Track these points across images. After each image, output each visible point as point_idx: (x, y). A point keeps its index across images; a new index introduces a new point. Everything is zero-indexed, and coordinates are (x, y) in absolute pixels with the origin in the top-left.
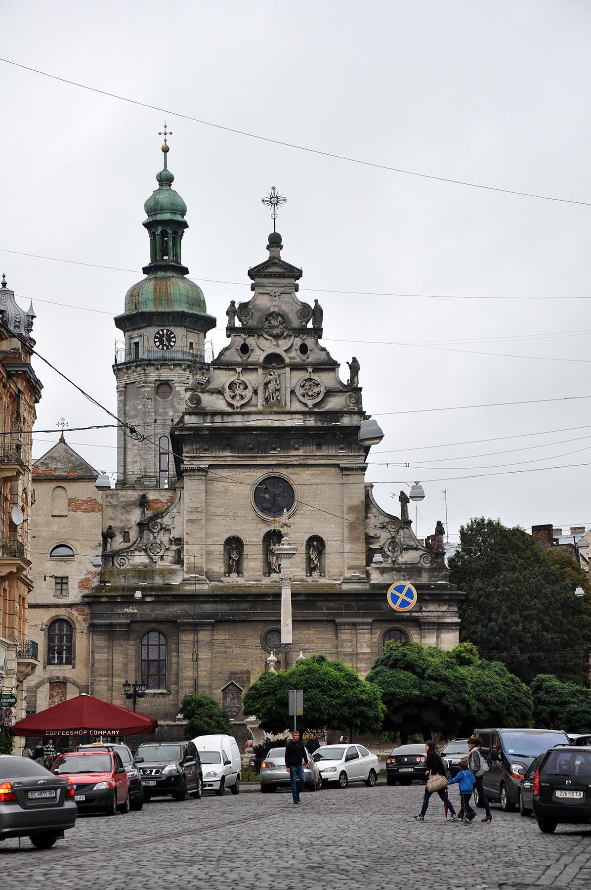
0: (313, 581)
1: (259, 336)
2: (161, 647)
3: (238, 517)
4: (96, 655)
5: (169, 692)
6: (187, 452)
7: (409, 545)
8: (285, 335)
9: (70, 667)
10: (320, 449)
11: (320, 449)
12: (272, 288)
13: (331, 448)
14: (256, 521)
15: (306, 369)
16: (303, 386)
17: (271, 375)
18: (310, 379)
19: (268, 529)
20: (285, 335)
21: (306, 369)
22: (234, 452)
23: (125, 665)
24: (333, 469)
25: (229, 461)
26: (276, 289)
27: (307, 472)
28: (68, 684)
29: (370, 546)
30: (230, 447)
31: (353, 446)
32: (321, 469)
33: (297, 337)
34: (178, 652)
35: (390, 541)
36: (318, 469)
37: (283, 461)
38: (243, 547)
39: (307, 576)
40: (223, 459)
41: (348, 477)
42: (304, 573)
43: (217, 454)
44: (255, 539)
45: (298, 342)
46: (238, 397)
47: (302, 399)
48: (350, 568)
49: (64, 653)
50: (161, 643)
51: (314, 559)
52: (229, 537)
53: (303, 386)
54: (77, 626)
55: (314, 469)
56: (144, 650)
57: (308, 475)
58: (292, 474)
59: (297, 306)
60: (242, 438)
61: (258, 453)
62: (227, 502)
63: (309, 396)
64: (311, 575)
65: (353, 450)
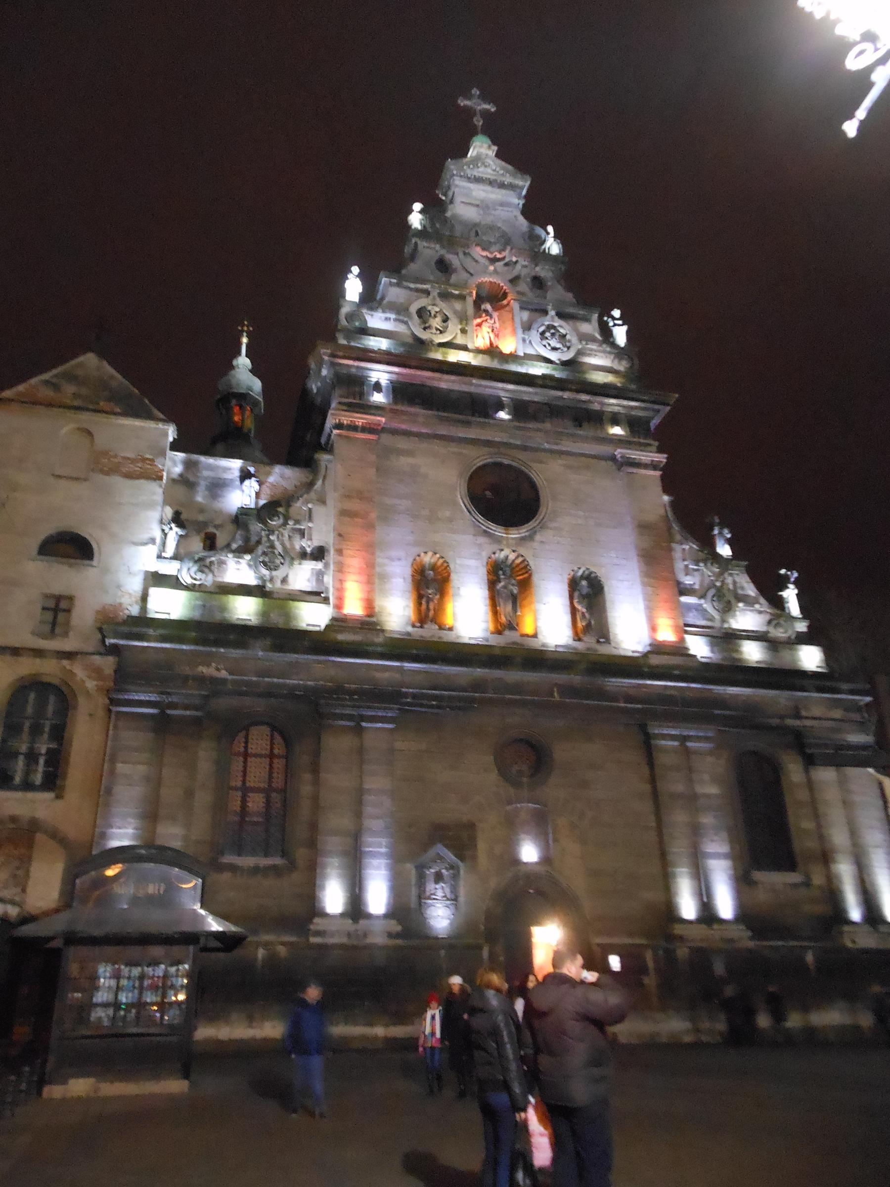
2: (276, 761)
4: (119, 766)
5: (292, 866)
6: (341, 396)
9: (49, 795)
10: (580, 426)
11: (580, 426)
18: (554, 327)
22: (431, 409)
23: (189, 794)
24: (603, 463)
27: (560, 462)
28: (40, 837)
34: (315, 769)
49: (42, 761)
50: (276, 751)
54: (82, 700)
56: (237, 765)
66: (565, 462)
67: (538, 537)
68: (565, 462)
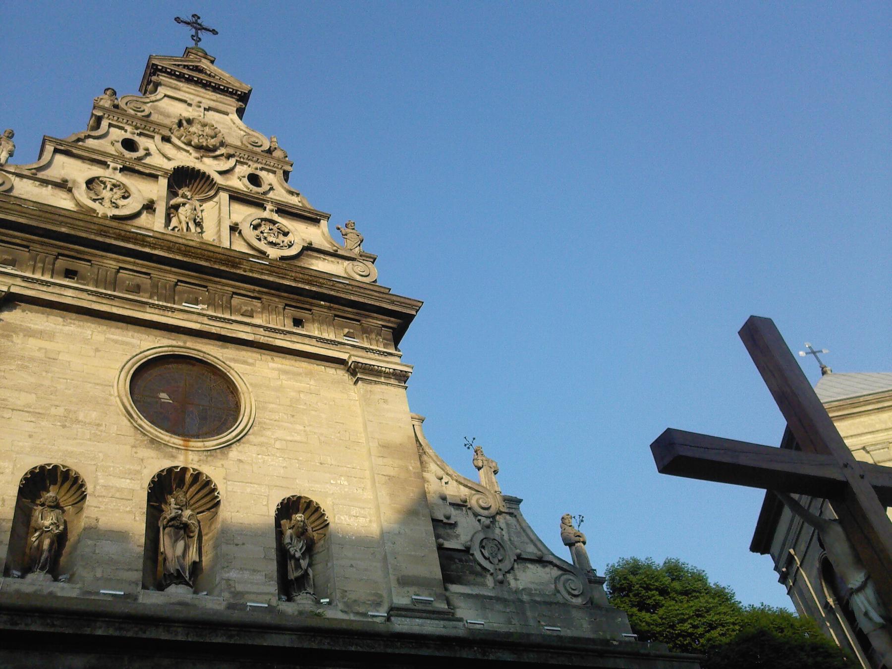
0: (301, 613)
1: (166, 139)
3: (78, 421)
7: (525, 552)
8: (218, 153)
10: (303, 327)
12: (192, 97)
13: (325, 327)
14: (131, 440)
15: (261, 206)
16: (256, 227)
17: (184, 196)
19: (167, 464)
20: (218, 153)
21: (265, 209)
24: (331, 371)
25: (69, 297)
26: (198, 99)
27: (271, 365)
29: (441, 540)
30: (70, 274)
31: (373, 336)
32: (304, 365)
33: (243, 163)
35: (481, 536)
36: (298, 364)
37: (215, 328)
38: (83, 498)
39: (280, 599)
40: (51, 289)
41: (369, 387)
42: (273, 588)
43: (37, 276)
44: (125, 483)
45: (243, 170)
46: (107, 203)
47: (256, 243)
48: (404, 582)
51: (298, 555)
52: (42, 468)
53: (256, 227)
55: (287, 362)
57: (273, 369)
58: (234, 360)
59: (239, 131)
60: (111, 262)
61: (151, 298)
62: (47, 383)
63: (272, 244)
64: (290, 599)
65: (374, 342)
66: (280, 366)
67: (234, 453)
68: (280, 366)
